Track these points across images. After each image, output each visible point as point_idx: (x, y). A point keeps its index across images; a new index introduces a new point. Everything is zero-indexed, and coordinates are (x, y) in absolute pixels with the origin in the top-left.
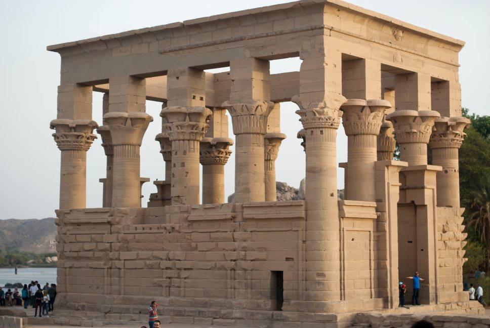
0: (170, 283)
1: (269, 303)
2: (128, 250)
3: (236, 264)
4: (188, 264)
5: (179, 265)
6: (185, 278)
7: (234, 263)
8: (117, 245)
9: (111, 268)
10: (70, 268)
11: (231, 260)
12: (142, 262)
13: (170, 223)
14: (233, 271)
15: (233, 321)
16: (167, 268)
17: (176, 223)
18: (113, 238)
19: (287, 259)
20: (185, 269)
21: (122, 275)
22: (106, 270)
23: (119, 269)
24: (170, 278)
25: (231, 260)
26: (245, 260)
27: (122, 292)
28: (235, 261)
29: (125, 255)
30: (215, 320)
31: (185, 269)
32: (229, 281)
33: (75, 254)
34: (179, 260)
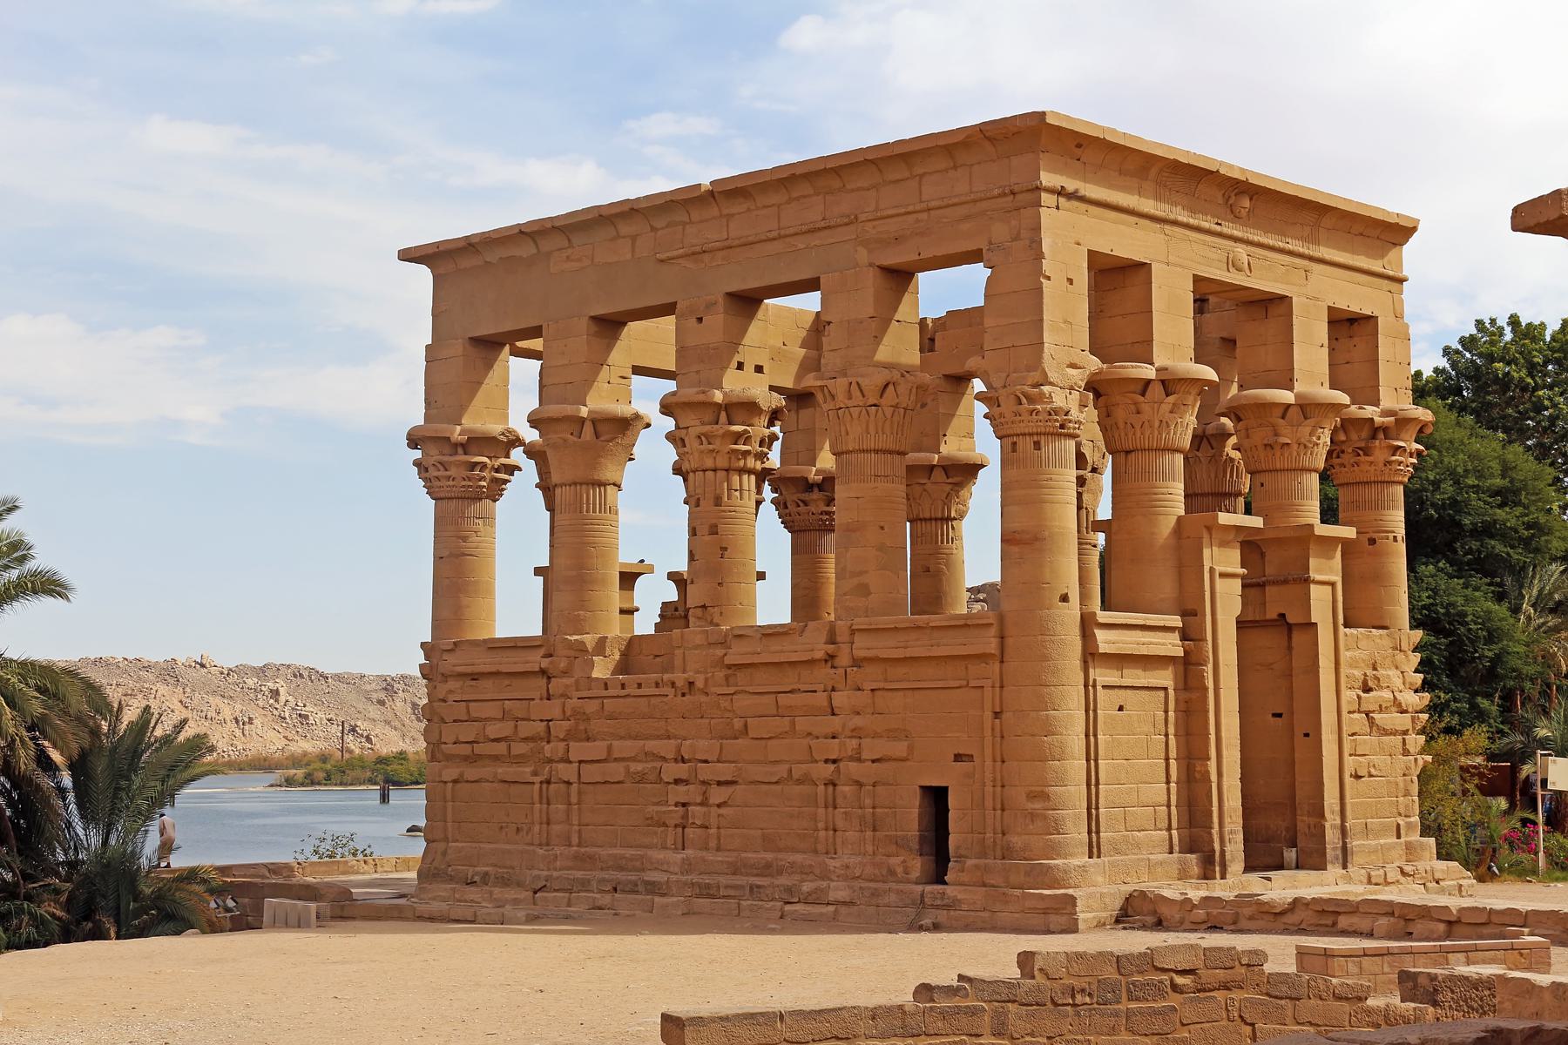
0: (685, 816)
1: (917, 866)
2: (588, 739)
3: (838, 770)
4: (725, 771)
5: (705, 772)
6: (719, 806)
7: (832, 767)
8: (559, 728)
9: (548, 782)
10: (455, 781)
11: (826, 761)
12: (620, 766)
13: (684, 671)
14: (831, 788)
15: (831, 908)
16: (677, 782)
17: (698, 672)
18: (553, 708)
19: (958, 758)
20: (719, 783)
21: (574, 799)
22: (537, 786)
23: (569, 783)
24: (684, 805)
25: (826, 761)
26: (859, 760)
27: (575, 840)
28: (834, 761)
29: (578, 750)
30: (788, 908)
31: (719, 783)
32: (821, 811)
33: (465, 750)
34: (706, 761)
